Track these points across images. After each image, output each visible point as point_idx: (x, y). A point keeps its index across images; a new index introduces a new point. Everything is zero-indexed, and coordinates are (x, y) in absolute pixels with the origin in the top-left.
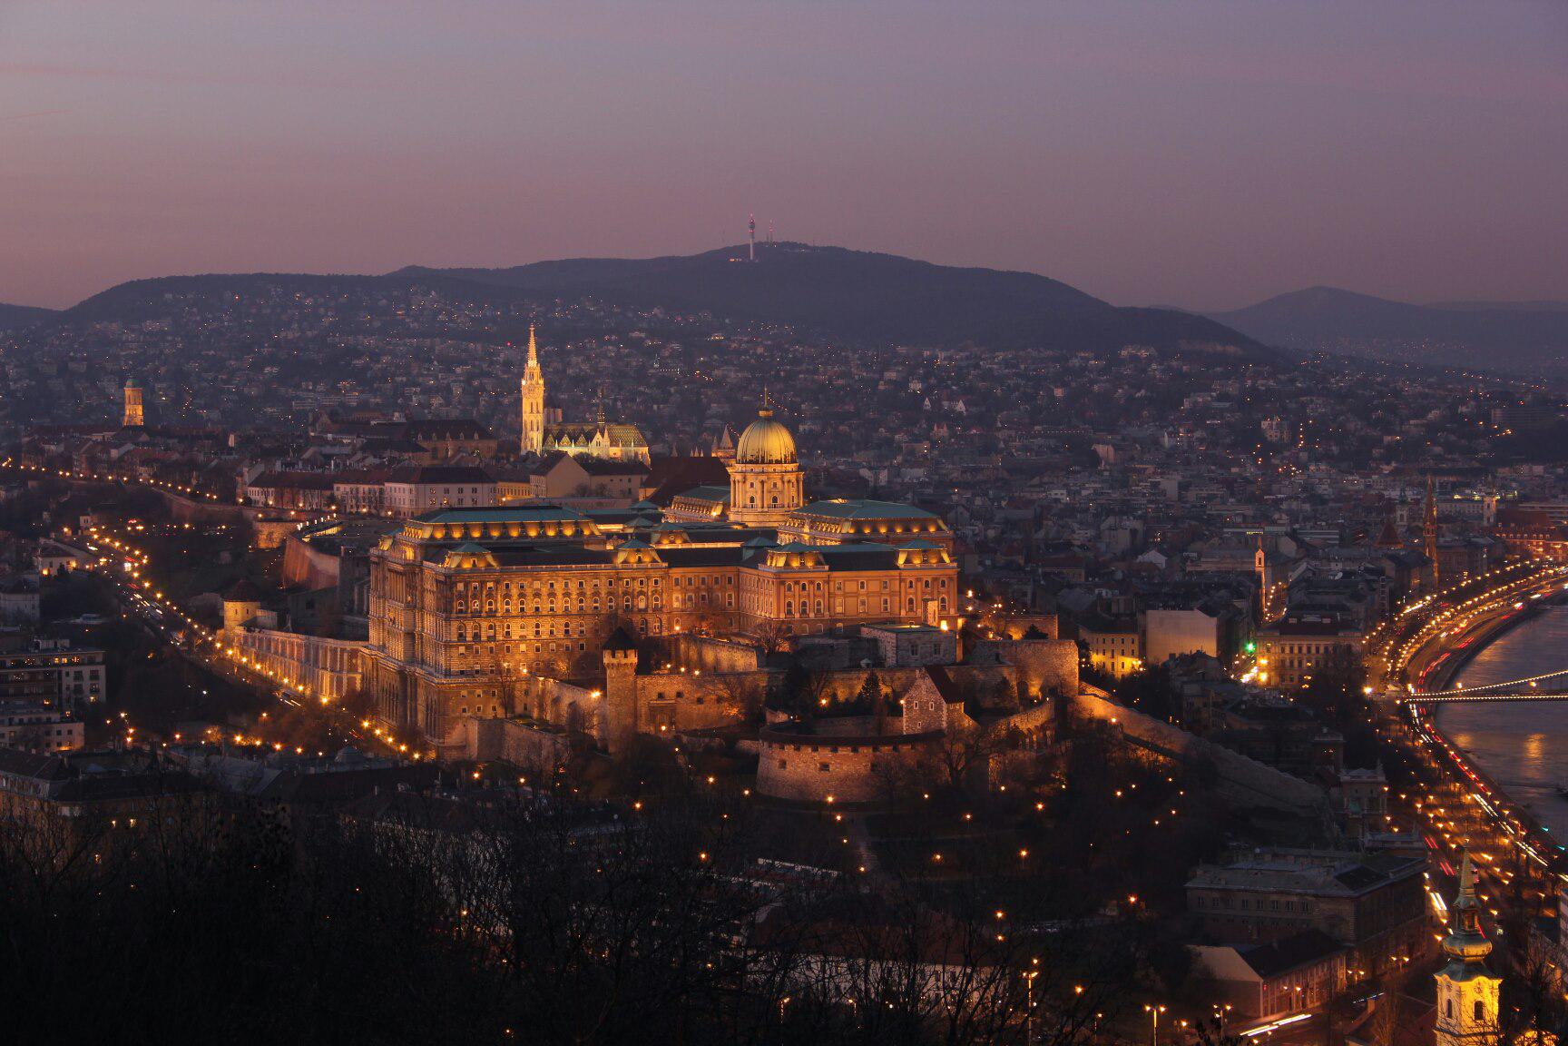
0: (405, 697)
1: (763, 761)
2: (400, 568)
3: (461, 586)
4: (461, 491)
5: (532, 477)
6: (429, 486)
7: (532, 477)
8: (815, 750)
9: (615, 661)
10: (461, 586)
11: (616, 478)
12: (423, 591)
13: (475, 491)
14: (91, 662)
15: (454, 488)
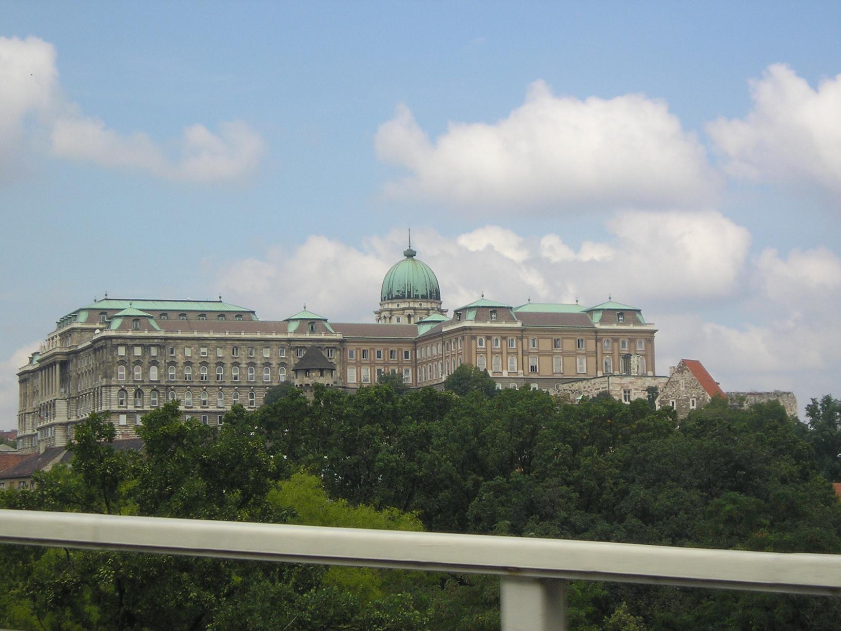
3: (122, 351)
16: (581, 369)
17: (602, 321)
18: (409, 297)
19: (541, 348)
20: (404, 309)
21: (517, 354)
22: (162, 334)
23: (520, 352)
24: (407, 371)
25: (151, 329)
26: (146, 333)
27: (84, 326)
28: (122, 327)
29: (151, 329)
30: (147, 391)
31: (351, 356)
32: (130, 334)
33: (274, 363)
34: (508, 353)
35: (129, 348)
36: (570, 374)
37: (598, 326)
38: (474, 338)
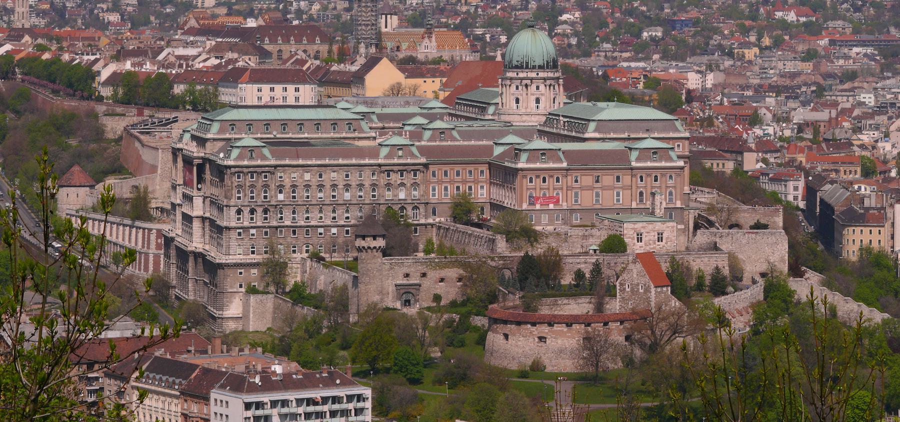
6: (256, 86)
13: (297, 90)
15: (279, 88)
16: (618, 200)
17: (638, 159)
18: (527, 67)
19: (583, 184)
21: (562, 189)
22: (273, 162)
23: (565, 188)
24: (482, 187)
25: (264, 158)
26: (259, 162)
27: (215, 137)
28: (240, 157)
29: (264, 158)
32: (246, 163)
33: (367, 184)
37: (634, 164)
38: (525, 177)
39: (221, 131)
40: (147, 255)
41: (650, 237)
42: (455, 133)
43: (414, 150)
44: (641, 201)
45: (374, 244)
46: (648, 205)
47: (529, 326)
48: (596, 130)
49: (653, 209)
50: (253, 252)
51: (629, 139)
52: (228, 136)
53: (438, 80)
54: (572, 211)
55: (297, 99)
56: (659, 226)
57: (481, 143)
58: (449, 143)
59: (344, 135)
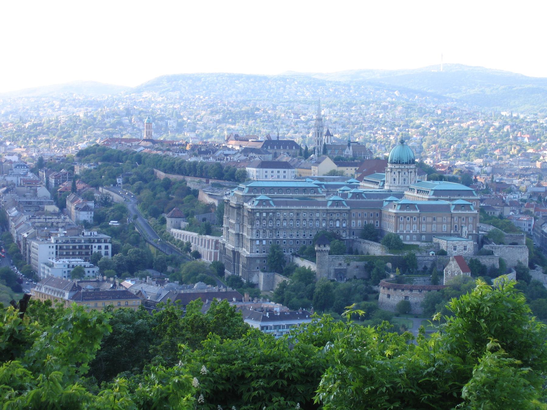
0: (234, 262)
1: (381, 296)
2: (234, 206)
3: (258, 215)
4: (278, 172)
5: (312, 167)
6: (265, 170)
7: (312, 167)
8: (403, 290)
9: (319, 249)
10: (258, 215)
11: (349, 168)
12: (243, 216)
13: (285, 172)
14: (105, 242)
17: (455, 209)
18: (400, 163)
19: (427, 221)
20: (397, 169)
21: (417, 224)
22: (275, 207)
25: (270, 205)
26: (268, 207)
28: (258, 205)
29: (270, 205)
30: (268, 231)
31: (354, 215)
32: (261, 208)
33: (321, 219)
34: (413, 223)
35: (261, 214)
36: (439, 231)
37: (452, 211)
39: (249, 192)
40: (211, 252)
41: (460, 248)
42: (363, 195)
43: (344, 203)
44: (456, 230)
45: (324, 249)
46: (459, 232)
47: (400, 291)
48: (434, 195)
49: (462, 234)
50: (264, 252)
51: (450, 200)
52: (252, 194)
53: (353, 168)
54: (422, 235)
55: (284, 177)
56: (465, 243)
57: (376, 200)
58: (361, 200)
59: (310, 195)
